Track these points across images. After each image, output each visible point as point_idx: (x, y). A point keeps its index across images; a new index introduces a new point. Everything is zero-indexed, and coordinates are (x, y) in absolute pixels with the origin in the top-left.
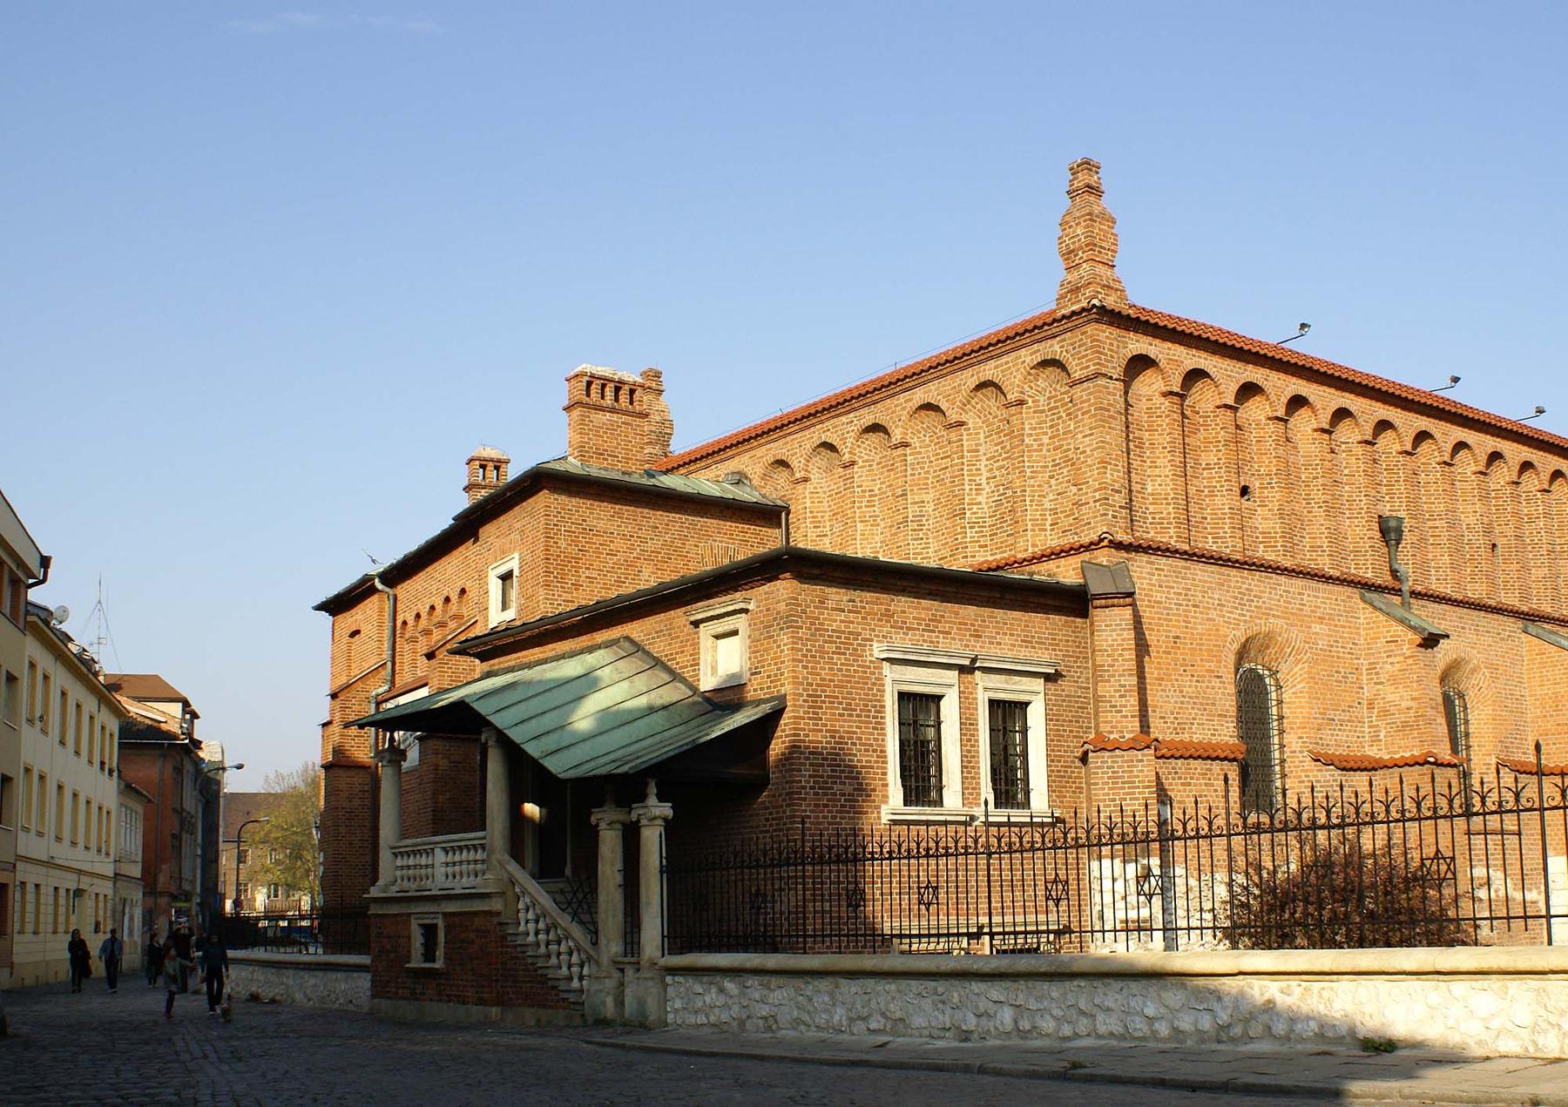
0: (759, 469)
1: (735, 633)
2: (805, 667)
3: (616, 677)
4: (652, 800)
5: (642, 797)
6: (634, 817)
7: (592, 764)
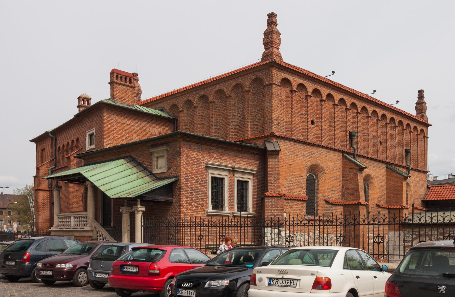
0: (169, 107)
1: (163, 156)
2: (185, 168)
3: (127, 168)
4: (139, 206)
5: (136, 205)
6: (133, 210)
7: (120, 194)
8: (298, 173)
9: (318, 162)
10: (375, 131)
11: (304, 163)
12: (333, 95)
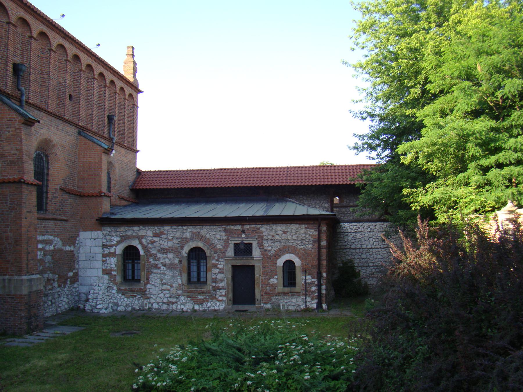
10: (62, 75)
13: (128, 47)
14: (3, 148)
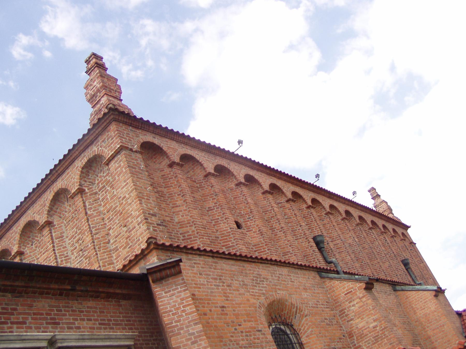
8: (249, 324)
9: (281, 294)
11: (252, 301)
12: (256, 177)
13: (369, 191)
14: (357, 328)
